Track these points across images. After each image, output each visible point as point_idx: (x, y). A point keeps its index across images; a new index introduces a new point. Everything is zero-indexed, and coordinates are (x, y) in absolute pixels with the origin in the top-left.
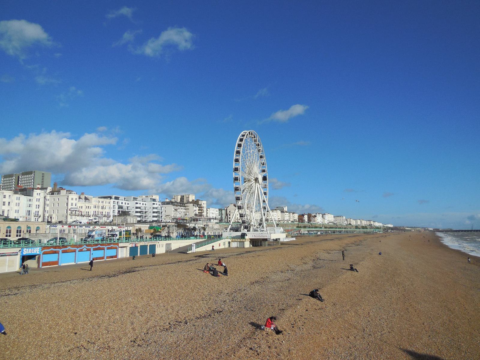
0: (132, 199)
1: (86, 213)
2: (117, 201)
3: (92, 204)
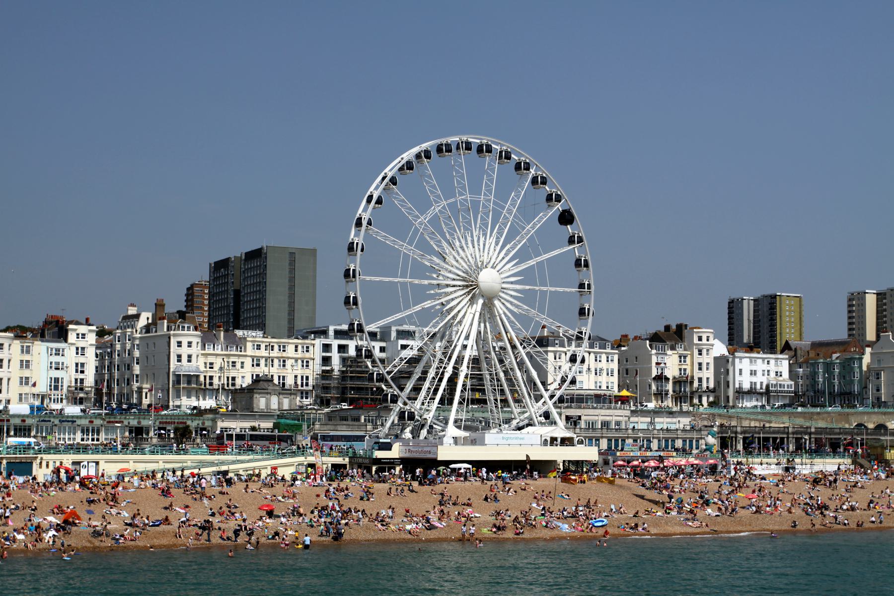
0: (394, 335)
1: (226, 382)
2: (335, 343)
3: (246, 356)
